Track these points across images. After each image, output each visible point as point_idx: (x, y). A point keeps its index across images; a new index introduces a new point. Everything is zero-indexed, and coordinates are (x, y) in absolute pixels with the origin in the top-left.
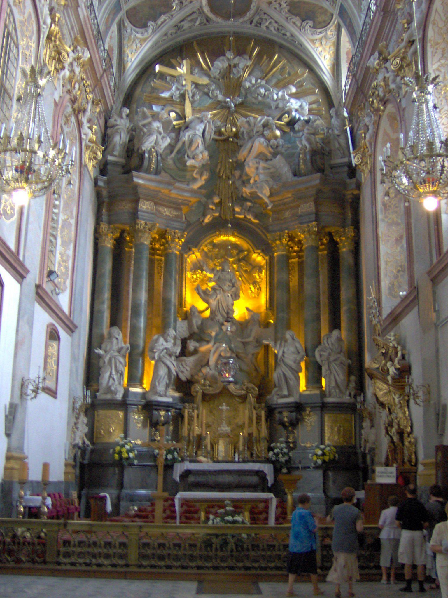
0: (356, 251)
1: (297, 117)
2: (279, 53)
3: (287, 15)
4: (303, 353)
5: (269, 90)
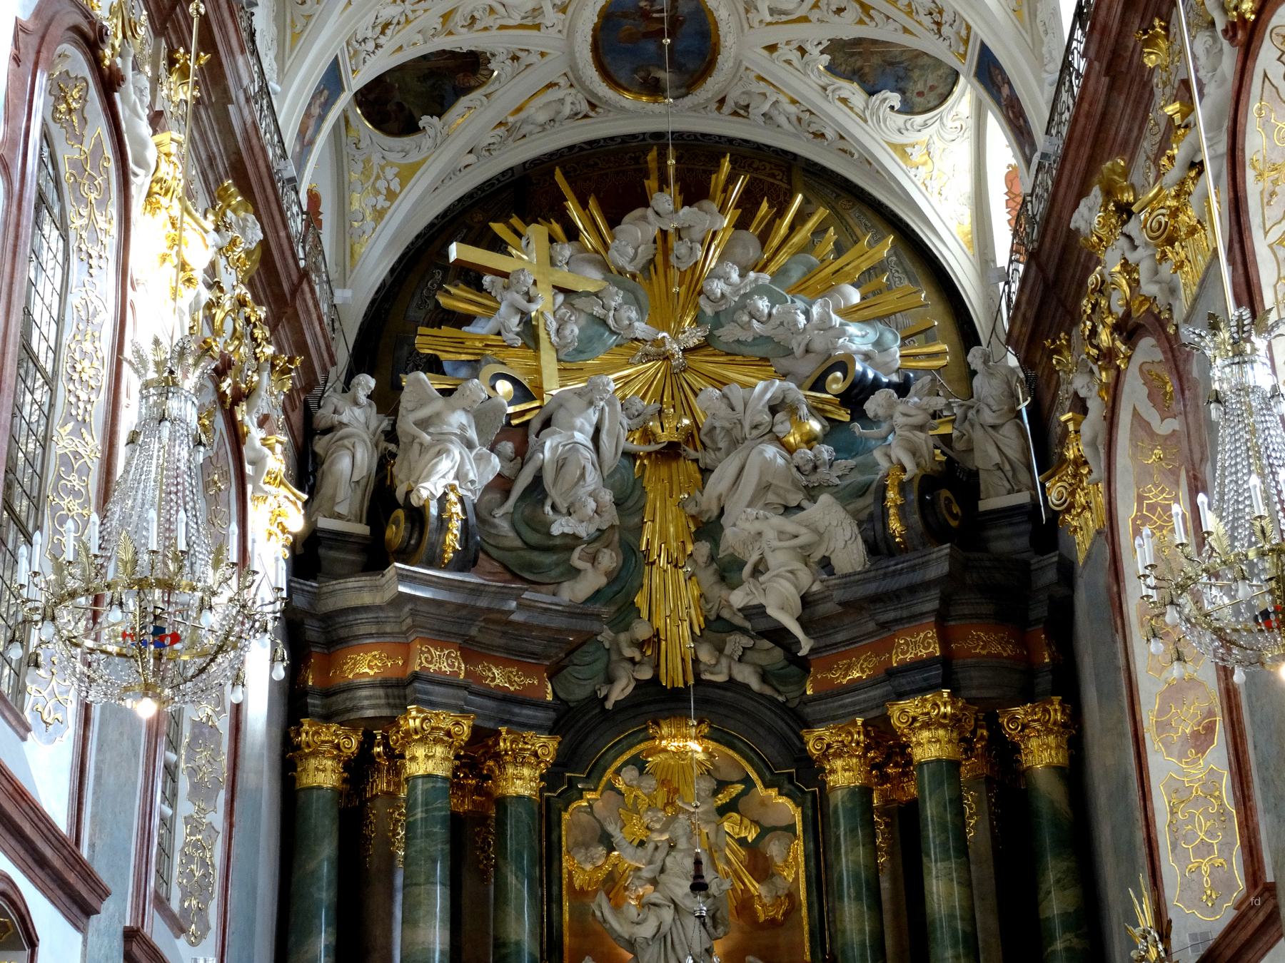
0: (1074, 772)
1: (871, 375)
2: (807, 189)
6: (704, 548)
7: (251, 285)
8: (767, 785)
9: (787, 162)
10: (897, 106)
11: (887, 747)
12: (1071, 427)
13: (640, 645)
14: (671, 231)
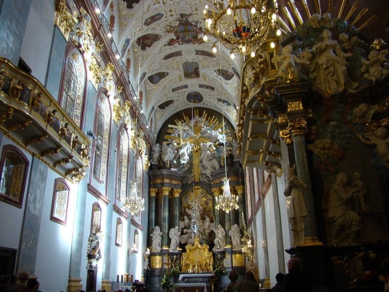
4: (224, 233)
6: (200, 164)
7: (143, 139)
9: (213, 111)
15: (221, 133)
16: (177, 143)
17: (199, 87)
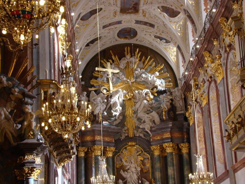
0: (189, 154)
3: (153, 39)
5: (147, 75)
6: (135, 116)
8: (145, 152)
9: (147, 48)
10: (165, 42)
11: (163, 150)
12: (189, 108)
13: (126, 131)
14: (129, 61)
15: (159, 77)
16: (106, 89)
17: (135, 23)
